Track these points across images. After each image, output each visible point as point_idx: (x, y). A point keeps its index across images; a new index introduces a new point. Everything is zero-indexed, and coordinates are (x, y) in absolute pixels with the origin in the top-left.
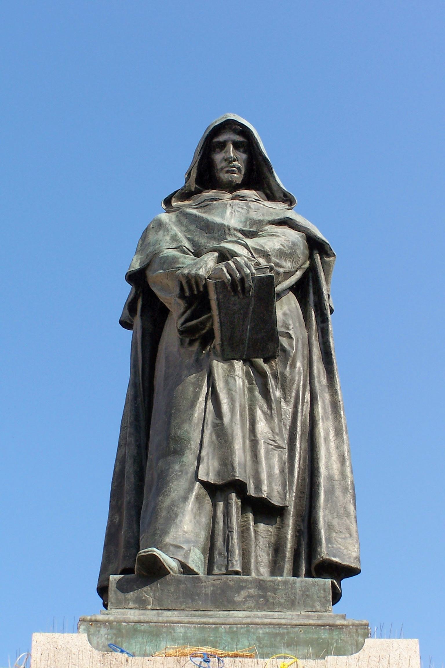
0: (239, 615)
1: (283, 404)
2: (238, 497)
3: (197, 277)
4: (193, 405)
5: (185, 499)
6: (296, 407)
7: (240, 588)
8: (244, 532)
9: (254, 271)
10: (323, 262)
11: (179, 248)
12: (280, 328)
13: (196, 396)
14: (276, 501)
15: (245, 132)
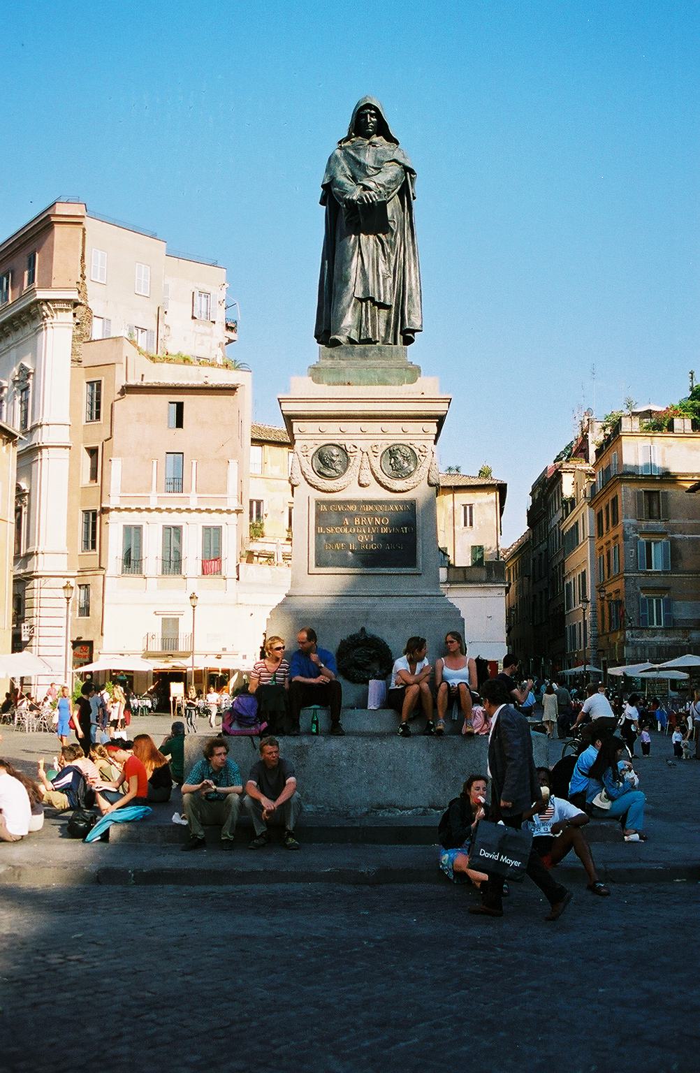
0: (369, 362)
1: (391, 255)
2: (371, 302)
3: (353, 200)
4: (352, 259)
5: (349, 306)
6: (396, 256)
7: (371, 349)
8: (373, 317)
9: (377, 198)
10: (411, 177)
11: (345, 176)
12: (389, 219)
13: (353, 253)
14: (388, 303)
15: (376, 109)
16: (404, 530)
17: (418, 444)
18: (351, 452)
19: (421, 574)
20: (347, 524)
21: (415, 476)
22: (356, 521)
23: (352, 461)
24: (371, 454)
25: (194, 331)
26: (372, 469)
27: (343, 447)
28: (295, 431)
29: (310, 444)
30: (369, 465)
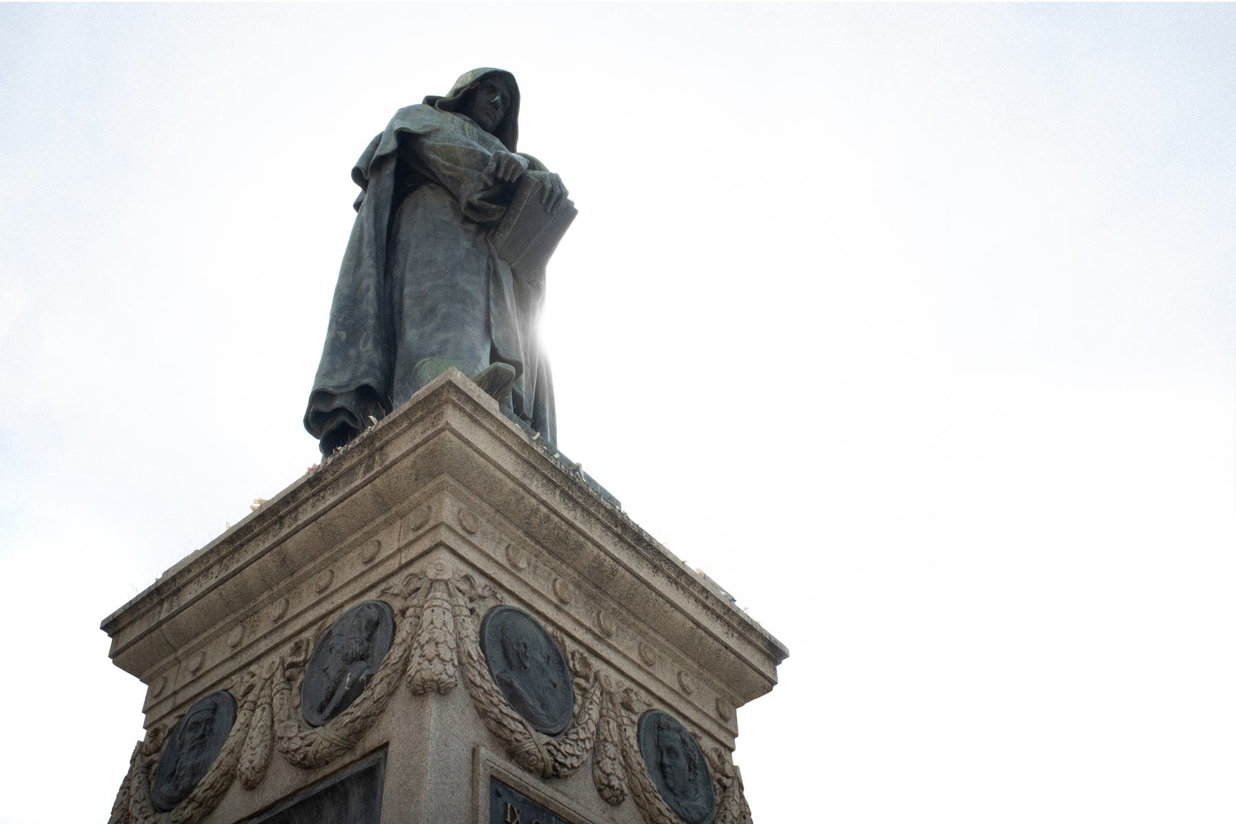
23: (579, 698)
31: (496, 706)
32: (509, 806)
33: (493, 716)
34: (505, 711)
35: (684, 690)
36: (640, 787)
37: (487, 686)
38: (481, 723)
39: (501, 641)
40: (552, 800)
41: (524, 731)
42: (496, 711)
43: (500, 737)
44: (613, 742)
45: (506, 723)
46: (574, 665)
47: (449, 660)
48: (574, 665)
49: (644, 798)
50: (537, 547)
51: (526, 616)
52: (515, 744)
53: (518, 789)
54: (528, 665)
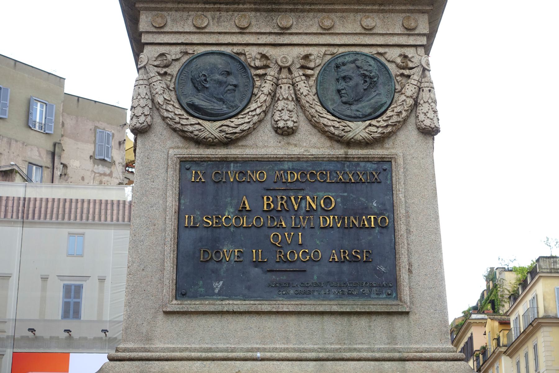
16: (369, 220)
17: (394, 54)
18: (257, 68)
19: (407, 313)
20: (248, 208)
21: (389, 113)
22: (266, 202)
23: (258, 83)
24: (297, 73)
25: (92, 171)
26: (298, 100)
27: (242, 58)
28: (143, 26)
29: (174, 52)
30: (292, 92)
31: (179, 123)
32: (194, 173)
33: (178, 129)
34: (184, 123)
35: (365, 29)
36: (310, 116)
37: (170, 115)
38: (175, 135)
39: (192, 79)
40: (228, 156)
41: (200, 127)
42: (178, 126)
43: (186, 137)
44: (283, 98)
45: (186, 129)
46: (255, 64)
47: (141, 114)
48: (255, 64)
49: (313, 121)
50: (216, 6)
51: (213, 53)
52: (196, 137)
53: (202, 160)
54: (207, 86)
